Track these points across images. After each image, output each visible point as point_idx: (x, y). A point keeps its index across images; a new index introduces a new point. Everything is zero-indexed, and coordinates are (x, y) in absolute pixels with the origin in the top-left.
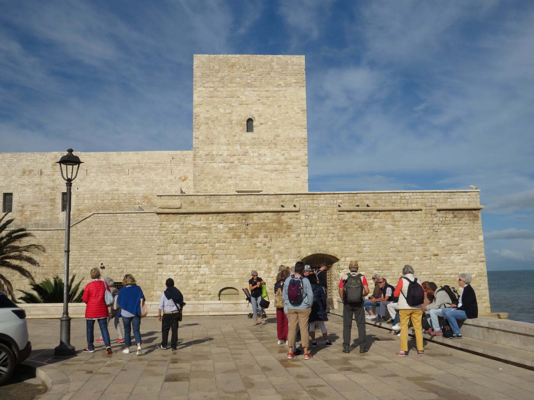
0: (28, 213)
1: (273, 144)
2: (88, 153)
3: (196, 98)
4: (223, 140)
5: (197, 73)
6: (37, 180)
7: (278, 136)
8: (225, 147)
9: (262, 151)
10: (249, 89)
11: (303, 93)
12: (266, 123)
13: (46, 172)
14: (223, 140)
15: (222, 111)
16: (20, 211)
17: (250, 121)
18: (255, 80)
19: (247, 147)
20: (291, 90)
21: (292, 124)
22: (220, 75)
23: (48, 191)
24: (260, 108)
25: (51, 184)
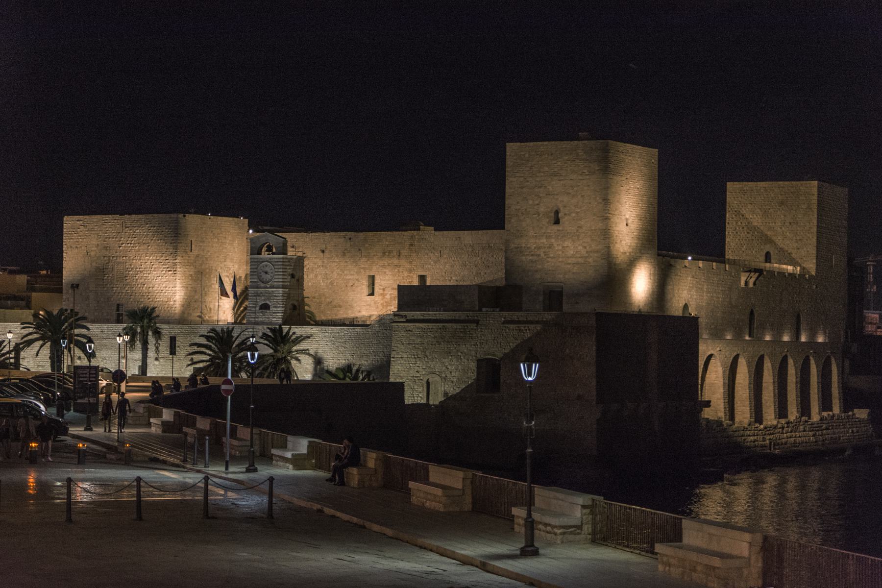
2: (441, 233)
7: (580, 227)
8: (532, 241)
9: (566, 244)
10: (556, 178)
12: (569, 214)
15: (531, 202)
16: (382, 294)
17: (557, 212)
18: (561, 168)
19: (553, 241)
21: (594, 215)
24: (566, 199)
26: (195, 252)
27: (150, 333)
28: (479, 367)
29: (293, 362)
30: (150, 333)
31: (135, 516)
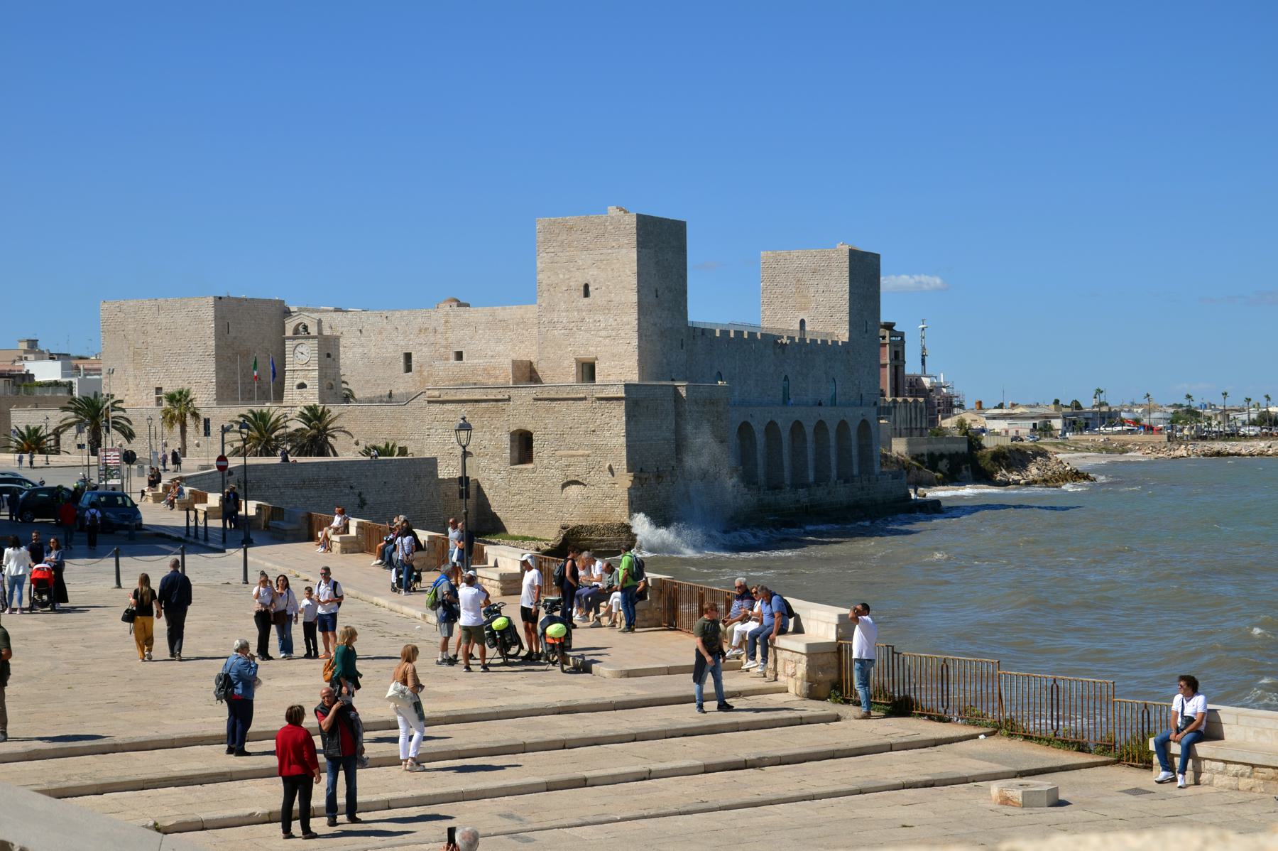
0: (425, 373)
1: (606, 309)
3: (539, 264)
4: (563, 306)
5: (540, 237)
6: (431, 338)
11: (634, 255)
13: (440, 329)
14: (563, 306)
17: (586, 287)
20: (624, 251)
22: (560, 238)
23: (442, 350)
25: (444, 343)
26: (233, 333)
27: (188, 415)
28: (512, 441)
29: (330, 439)
30: (188, 415)
31: (114, 584)
